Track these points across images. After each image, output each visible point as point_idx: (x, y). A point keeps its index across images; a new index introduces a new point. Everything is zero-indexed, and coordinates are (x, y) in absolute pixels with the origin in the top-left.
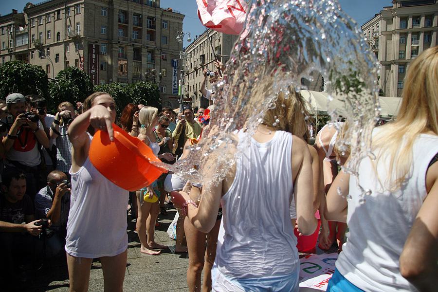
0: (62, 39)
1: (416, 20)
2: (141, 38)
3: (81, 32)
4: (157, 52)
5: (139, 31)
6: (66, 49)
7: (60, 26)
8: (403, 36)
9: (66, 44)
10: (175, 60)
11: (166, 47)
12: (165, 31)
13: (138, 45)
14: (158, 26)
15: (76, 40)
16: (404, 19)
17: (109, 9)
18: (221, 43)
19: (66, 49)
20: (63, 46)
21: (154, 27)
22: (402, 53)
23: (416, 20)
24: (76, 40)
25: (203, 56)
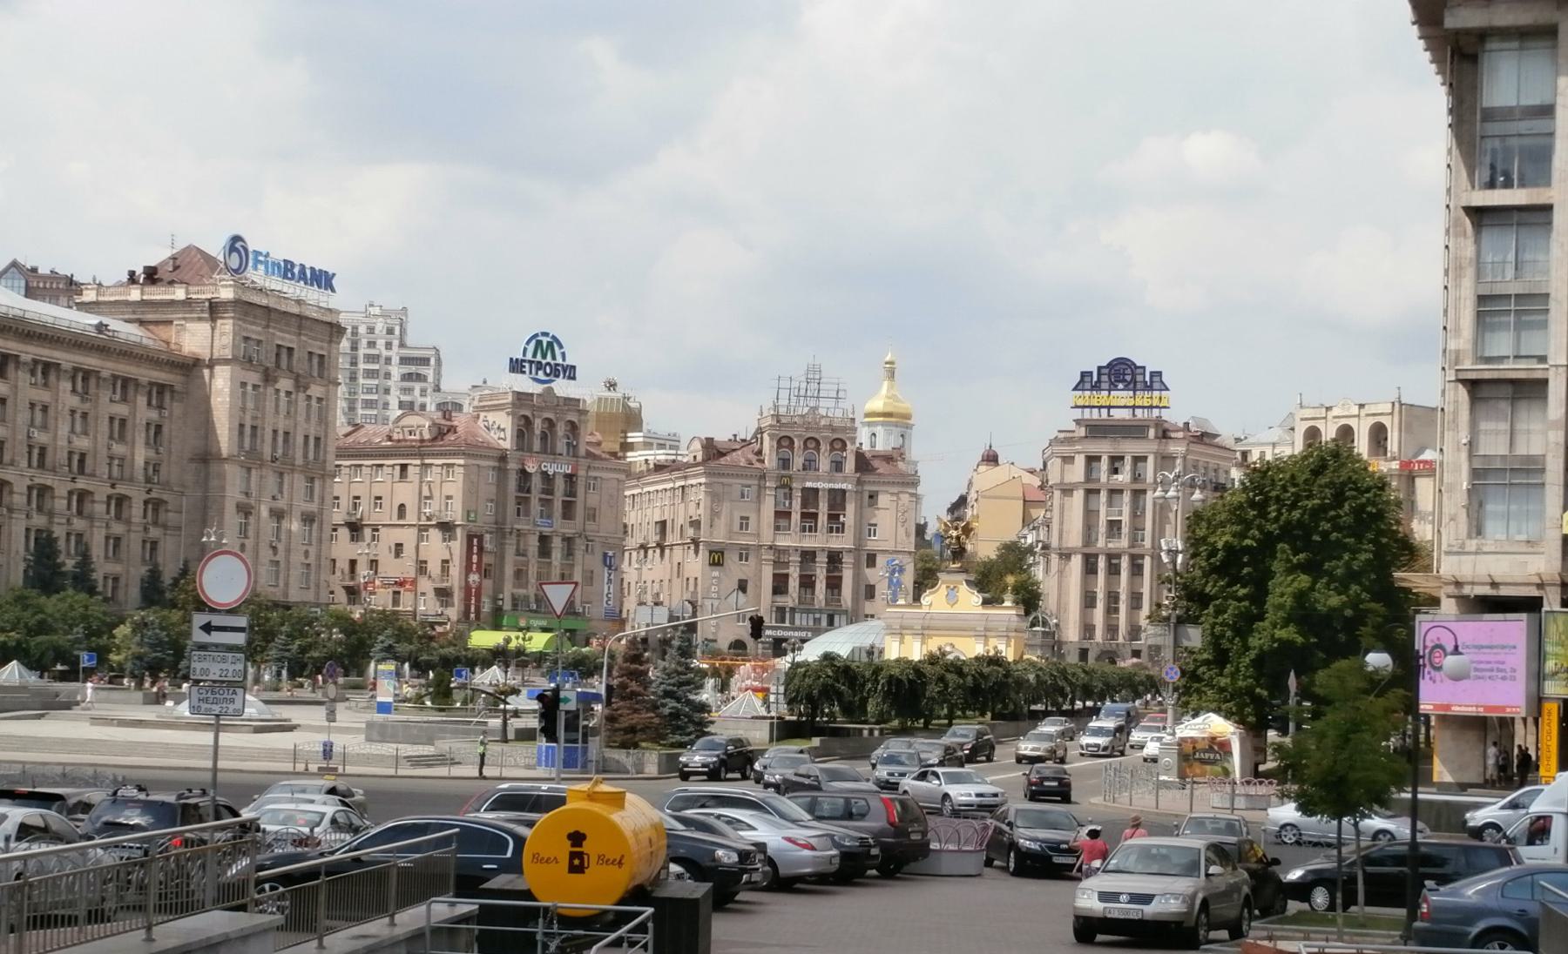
0: (411, 518)
1: (1116, 462)
2: (550, 516)
3: (456, 514)
4: (578, 541)
5: (546, 503)
6: (420, 539)
7: (406, 493)
8: (1091, 493)
9: (423, 529)
10: (610, 553)
11: (594, 527)
12: (593, 500)
13: (547, 530)
14: (580, 490)
15: (446, 528)
16: (1092, 460)
17: (499, 469)
18: (701, 511)
19: (420, 539)
20: (414, 531)
21: (574, 496)
23: (1116, 462)
24: (446, 528)
25: (663, 524)
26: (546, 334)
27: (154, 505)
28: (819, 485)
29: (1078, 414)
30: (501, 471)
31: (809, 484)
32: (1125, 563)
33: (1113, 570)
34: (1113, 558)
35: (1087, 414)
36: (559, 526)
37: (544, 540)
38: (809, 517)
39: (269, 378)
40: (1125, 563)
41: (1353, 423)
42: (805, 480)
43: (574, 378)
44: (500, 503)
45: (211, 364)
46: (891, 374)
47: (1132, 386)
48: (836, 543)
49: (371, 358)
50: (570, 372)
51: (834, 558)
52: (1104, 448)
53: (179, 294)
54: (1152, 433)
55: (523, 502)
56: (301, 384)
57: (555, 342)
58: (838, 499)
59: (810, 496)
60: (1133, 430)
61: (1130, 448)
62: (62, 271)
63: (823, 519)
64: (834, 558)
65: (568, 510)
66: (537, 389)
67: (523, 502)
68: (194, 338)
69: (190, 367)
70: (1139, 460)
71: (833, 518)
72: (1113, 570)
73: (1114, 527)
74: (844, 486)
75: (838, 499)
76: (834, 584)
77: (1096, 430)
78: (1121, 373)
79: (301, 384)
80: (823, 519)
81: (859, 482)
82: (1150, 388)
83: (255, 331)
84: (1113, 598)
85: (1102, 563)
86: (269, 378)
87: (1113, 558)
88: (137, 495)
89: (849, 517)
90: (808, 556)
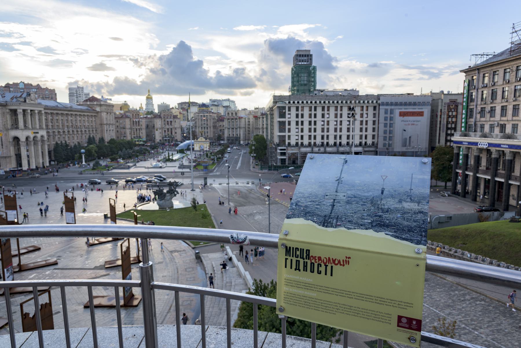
22: (202, 125)
27: (96, 130)
30: (131, 121)
34: (204, 128)
36: (138, 127)
37: (136, 129)
38: (168, 124)
39: (107, 113)
44: (131, 125)
45: (101, 112)
46: (149, 92)
48: (171, 127)
49: (80, 94)
51: (171, 129)
53: (95, 103)
55: (133, 124)
56: (110, 114)
58: (171, 122)
59: (168, 121)
62: (29, 83)
64: (171, 129)
65: (139, 125)
67: (133, 124)
68: (98, 109)
69: (98, 112)
75: (171, 122)
76: (171, 133)
79: (110, 114)
83: (105, 108)
86: (107, 113)
87: (204, 128)
88: (94, 130)
89: (173, 124)
90: (168, 129)
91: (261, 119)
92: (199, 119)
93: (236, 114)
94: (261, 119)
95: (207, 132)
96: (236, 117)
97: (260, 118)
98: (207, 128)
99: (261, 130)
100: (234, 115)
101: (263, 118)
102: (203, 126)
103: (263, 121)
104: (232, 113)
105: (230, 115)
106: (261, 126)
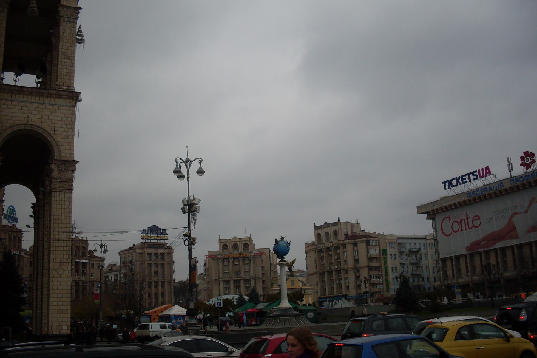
26: (12, 206)
28: (80, 261)
29: (142, 241)
31: (77, 260)
32: (160, 284)
33: (156, 286)
35: (144, 241)
40: (160, 284)
41: (238, 243)
42: (76, 259)
43: (17, 222)
47: (157, 234)
50: (16, 220)
52: (152, 251)
54: (166, 247)
57: (14, 210)
60: (162, 246)
61: (160, 251)
63: (81, 271)
66: (10, 225)
70: (162, 254)
71: (83, 271)
72: (156, 286)
73: (156, 273)
74: (86, 261)
77: (151, 246)
78: (154, 229)
80: (81, 271)
81: (89, 261)
82: (162, 234)
84: (156, 294)
85: (153, 284)
87: (156, 283)
89: (87, 271)
91: (349, 248)
92: (142, 263)
93: (246, 246)
94: (349, 248)
95: (163, 295)
96: (246, 254)
97: (344, 246)
98: (163, 283)
99: (351, 275)
100: (241, 249)
101: (355, 245)
102: (154, 278)
103: (356, 252)
104: (235, 246)
105: (230, 248)
106: (350, 263)
